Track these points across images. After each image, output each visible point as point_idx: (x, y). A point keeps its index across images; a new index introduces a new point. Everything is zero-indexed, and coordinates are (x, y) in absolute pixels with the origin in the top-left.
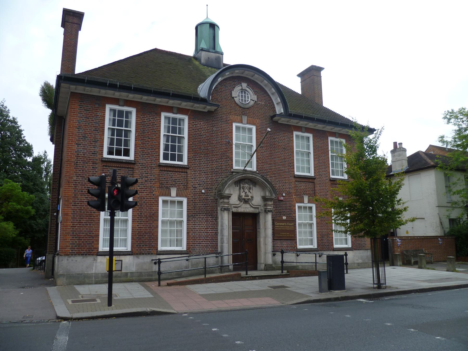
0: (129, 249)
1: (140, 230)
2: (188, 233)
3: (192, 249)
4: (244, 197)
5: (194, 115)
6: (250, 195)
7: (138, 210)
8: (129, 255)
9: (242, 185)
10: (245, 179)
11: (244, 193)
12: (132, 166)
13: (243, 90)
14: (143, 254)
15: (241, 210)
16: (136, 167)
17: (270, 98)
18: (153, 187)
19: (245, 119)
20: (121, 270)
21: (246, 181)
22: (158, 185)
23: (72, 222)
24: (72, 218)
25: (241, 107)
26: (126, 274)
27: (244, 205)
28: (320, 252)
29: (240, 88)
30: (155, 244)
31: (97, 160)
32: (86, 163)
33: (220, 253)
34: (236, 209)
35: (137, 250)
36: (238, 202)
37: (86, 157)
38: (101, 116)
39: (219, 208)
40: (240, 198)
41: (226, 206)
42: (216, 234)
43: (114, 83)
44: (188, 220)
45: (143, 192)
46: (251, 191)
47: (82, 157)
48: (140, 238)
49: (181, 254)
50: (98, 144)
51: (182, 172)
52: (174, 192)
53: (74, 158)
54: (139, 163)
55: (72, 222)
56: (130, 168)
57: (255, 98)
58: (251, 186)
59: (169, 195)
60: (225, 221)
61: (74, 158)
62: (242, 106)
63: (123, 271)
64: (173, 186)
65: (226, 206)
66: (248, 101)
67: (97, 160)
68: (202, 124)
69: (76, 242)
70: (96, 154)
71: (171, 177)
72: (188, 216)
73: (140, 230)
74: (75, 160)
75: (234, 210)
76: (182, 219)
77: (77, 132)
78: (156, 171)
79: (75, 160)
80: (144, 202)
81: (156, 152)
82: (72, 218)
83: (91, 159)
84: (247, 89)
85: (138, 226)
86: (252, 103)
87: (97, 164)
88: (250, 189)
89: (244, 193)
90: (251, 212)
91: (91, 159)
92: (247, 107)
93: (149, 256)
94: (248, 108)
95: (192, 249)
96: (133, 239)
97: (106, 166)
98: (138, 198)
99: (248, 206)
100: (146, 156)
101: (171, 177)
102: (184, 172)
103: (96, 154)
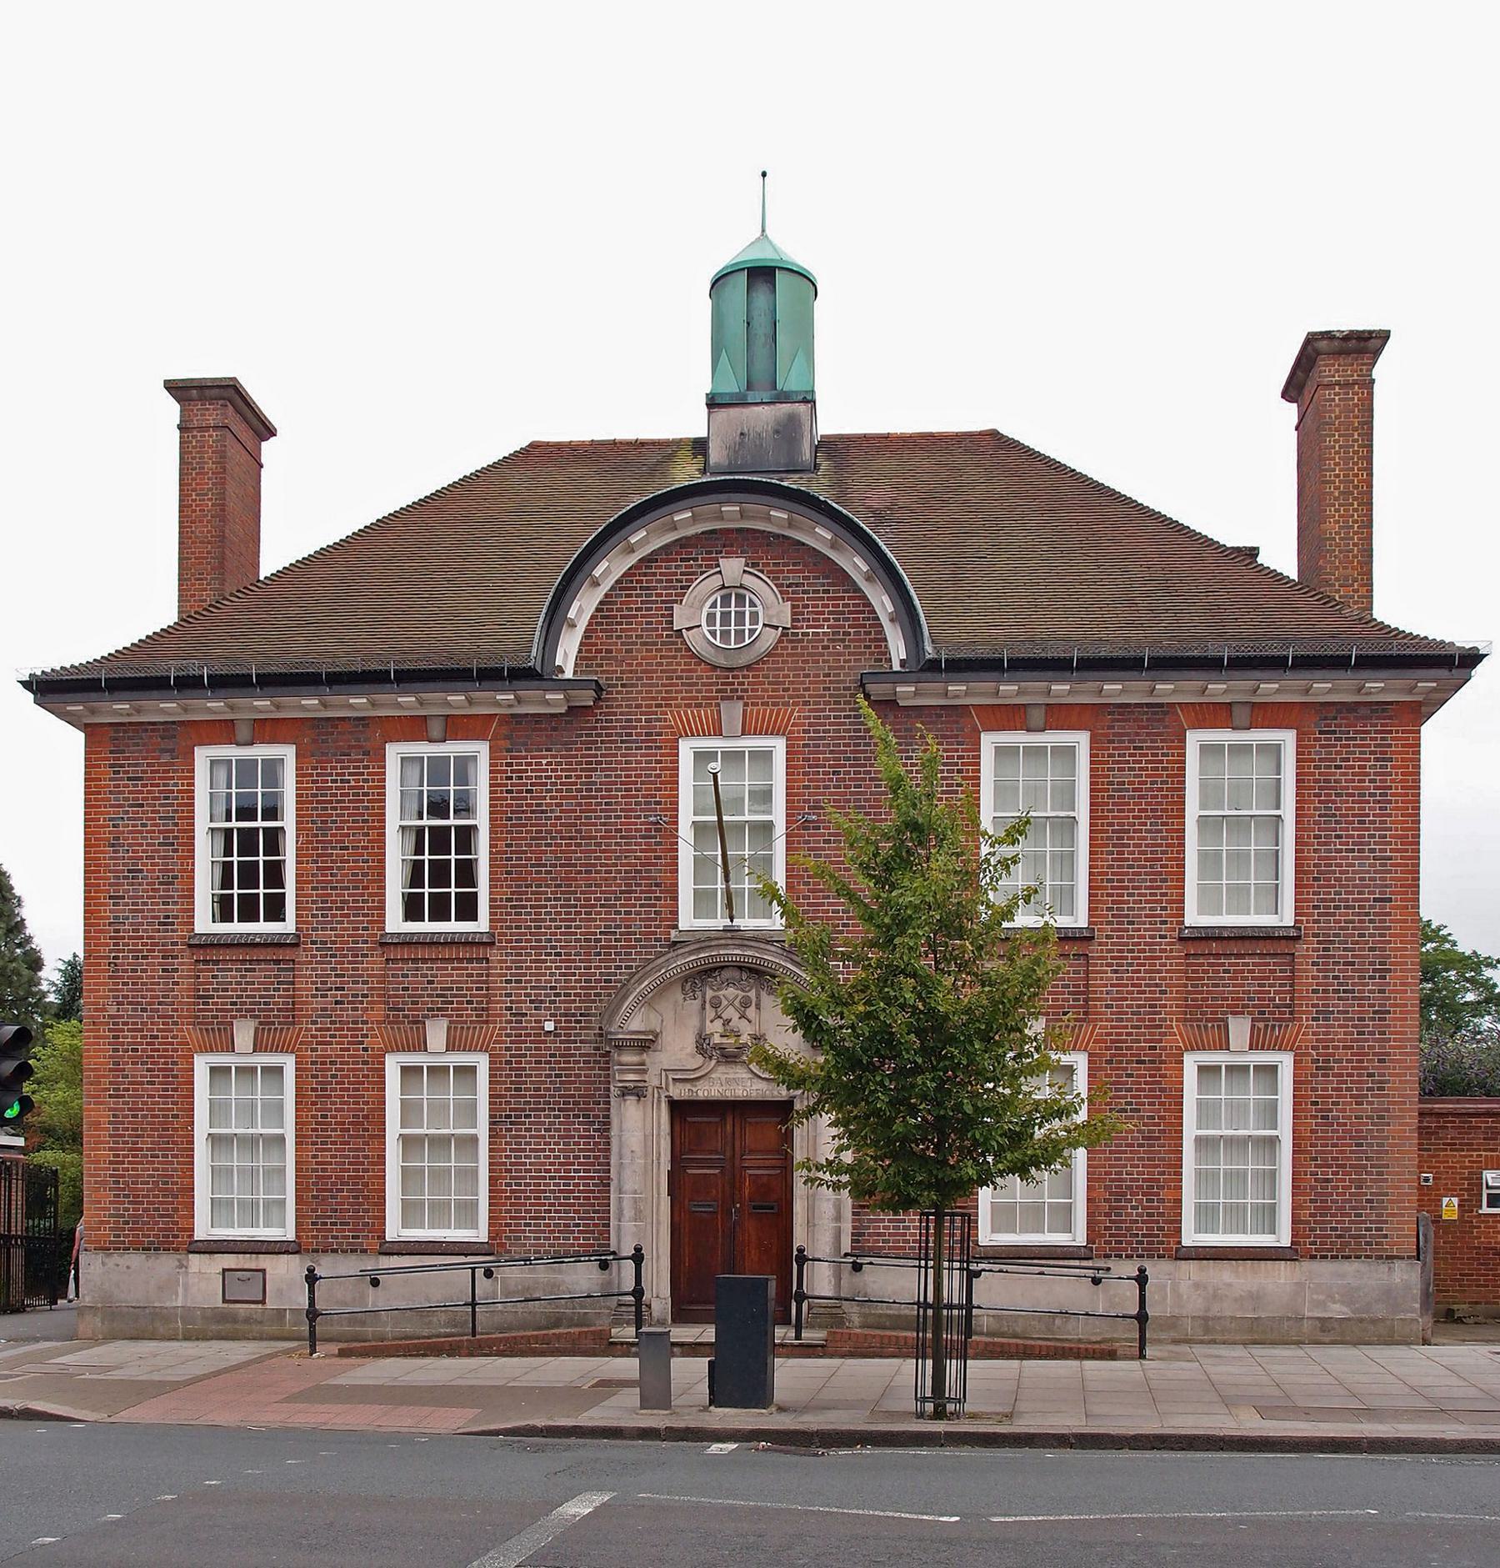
0: (291, 1235)
1: (323, 1170)
2: (493, 1180)
3: (509, 1238)
4: (717, 1039)
5: (511, 735)
6: (746, 1031)
7: (314, 1103)
8: (287, 1252)
9: (710, 993)
10: (720, 968)
11: (719, 1023)
12: (286, 954)
13: (733, 594)
14: (335, 1251)
15: (707, 1091)
16: (301, 955)
17: (865, 597)
18: (366, 1022)
19: (732, 713)
20: (263, 1302)
21: (726, 974)
22: (379, 1012)
23: (111, 1149)
24: (111, 1136)
25: (715, 668)
26: (280, 1313)
27: (722, 1069)
28: (1101, 1263)
29: (716, 581)
30: (375, 1217)
31: (176, 944)
32: (144, 957)
33: (614, 1253)
34: (688, 1086)
35: (316, 1237)
36: (699, 1060)
37: (142, 938)
38: (179, 791)
39: (614, 1091)
40: (703, 1045)
41: (631, 1077)
42: (605, 1183)
43: (191, 673)
44: (494, 1135)
45: (330, 1043)
46: (751, 1012)
47: (130, 938)
48: (325, 1198)
49: (466, 1255)
50: (176, 891)
51: (470, 960)
52: (437, 1033)
53: (108, 945)
54: (313, 943)
55: (111, 1149)
56: (286, 961)
57: (783, 614)
58: (752, 994)
59: (421, 1046)
60: (640, 1136)
61: (108, 945)
62: (723, 662)
63: (271, 1304)
64: (436, 1012)
65: (631, 1077)
66: (752, 632)
67: (176, 944)
68: (544, 765)
69: (127, 1210)
70: (173, 924)
71: (429, 982)
72: (493, 1123)
73: (323, 1170)
74: (111, 951)
75: (680, 1092)
76: (472, 1131)
77: (111, 858)
78: (374, 964)
79: (111, 951)
80: (333, 1076)
81: (370, 895)
82: (111, 1136)
83: (157, 944)
84: (749, 581)
85: (315, 1157)
86: (772, 636)
87: (176, 957)
88: (746, 1003)
89: (719, 1023)
90: (754, 1096)
91: (157, 944)
92: (743, 660)
93: (353, 1257)
94: (748, 667)
95: (509, 1238)
96: (299, 1200)
97: (206, 962)
98: (313, 1063)
99: (740, 1073)
100: (335, 916)
101: (429, 982)
102: (479, 960)
103: (173, 924)
